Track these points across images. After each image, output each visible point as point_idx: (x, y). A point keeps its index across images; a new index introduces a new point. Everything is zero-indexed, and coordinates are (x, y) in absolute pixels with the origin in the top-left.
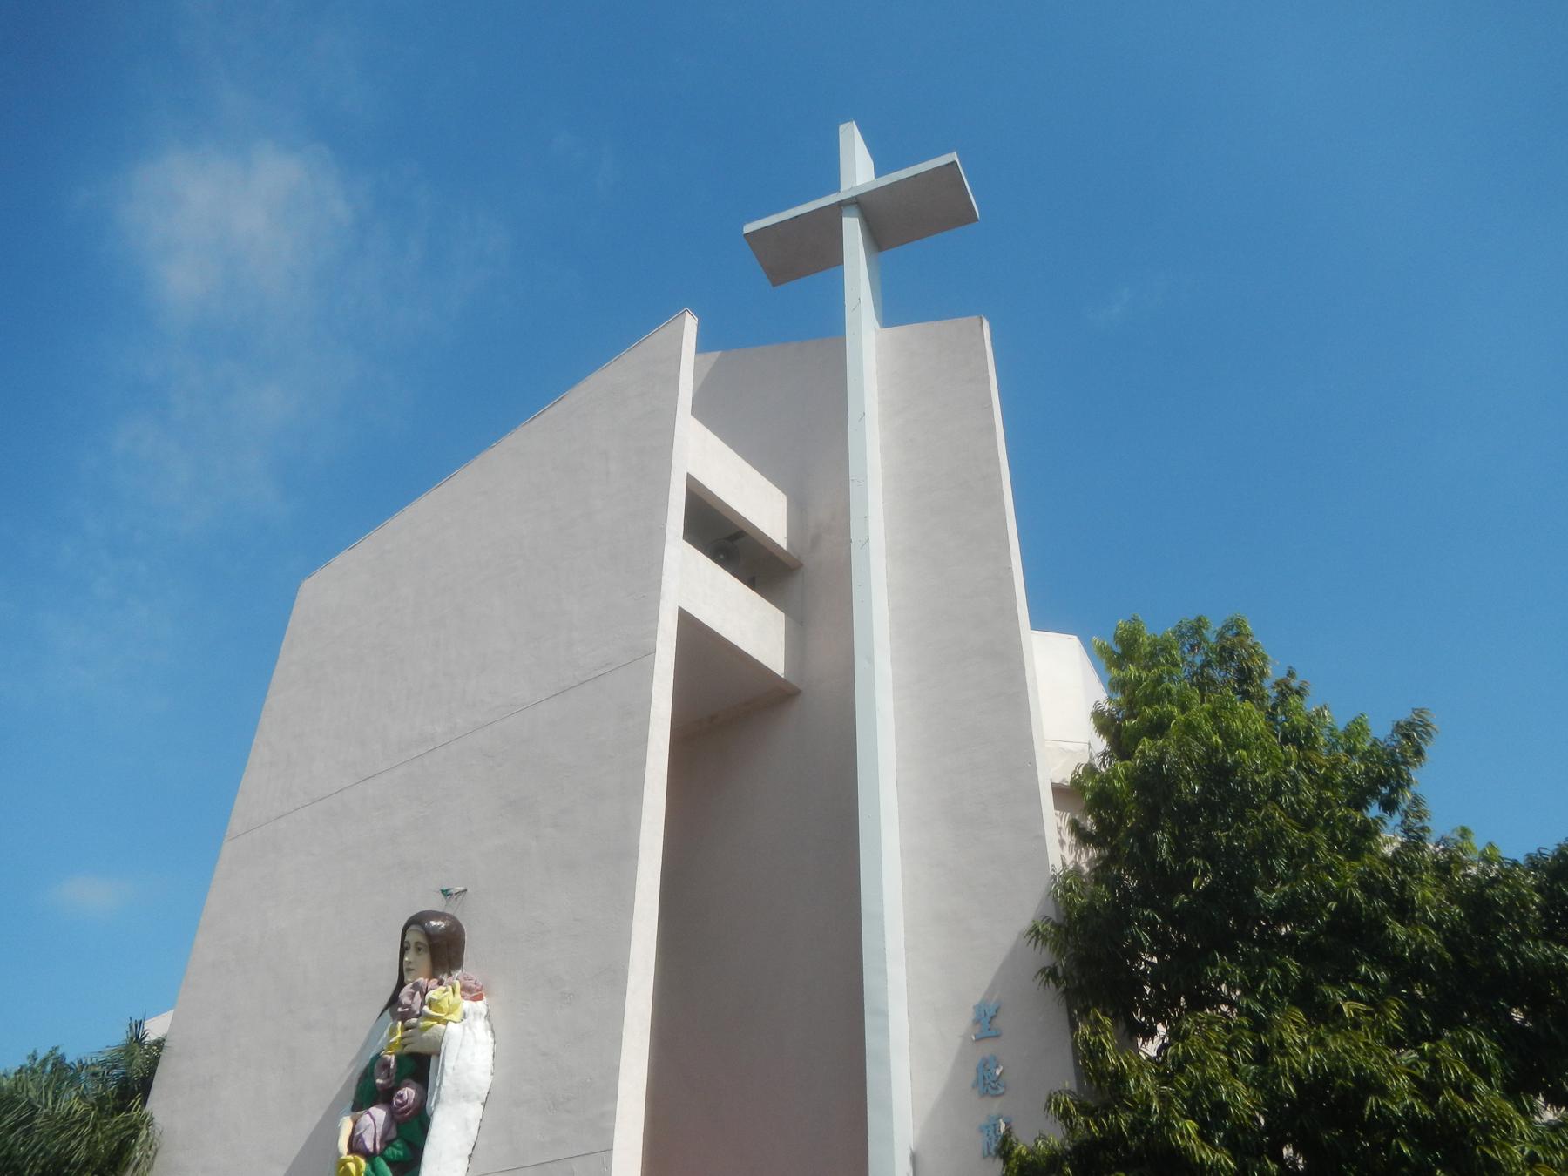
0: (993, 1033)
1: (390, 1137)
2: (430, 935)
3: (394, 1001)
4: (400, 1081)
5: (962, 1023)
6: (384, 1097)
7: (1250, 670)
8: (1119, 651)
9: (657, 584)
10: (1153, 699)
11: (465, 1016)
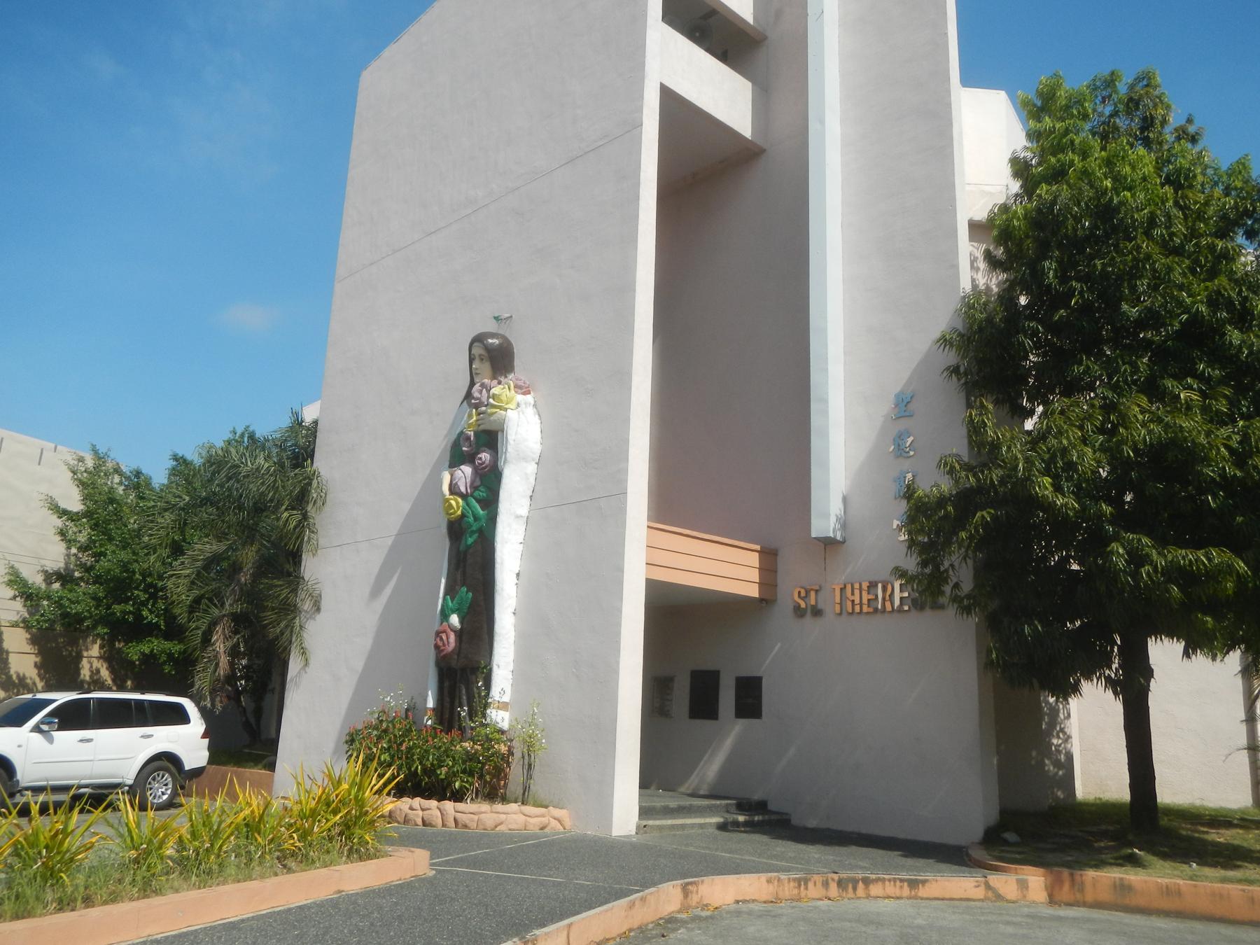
2: (488, 349)
3: (468, 395)
4: (479, 447)
5: (885, 407)
6: (470, 459)
7: (1152, 118)
8: (1039, 103)
9: (641, 66)
10: (1058, 149)
11: (518, 405)
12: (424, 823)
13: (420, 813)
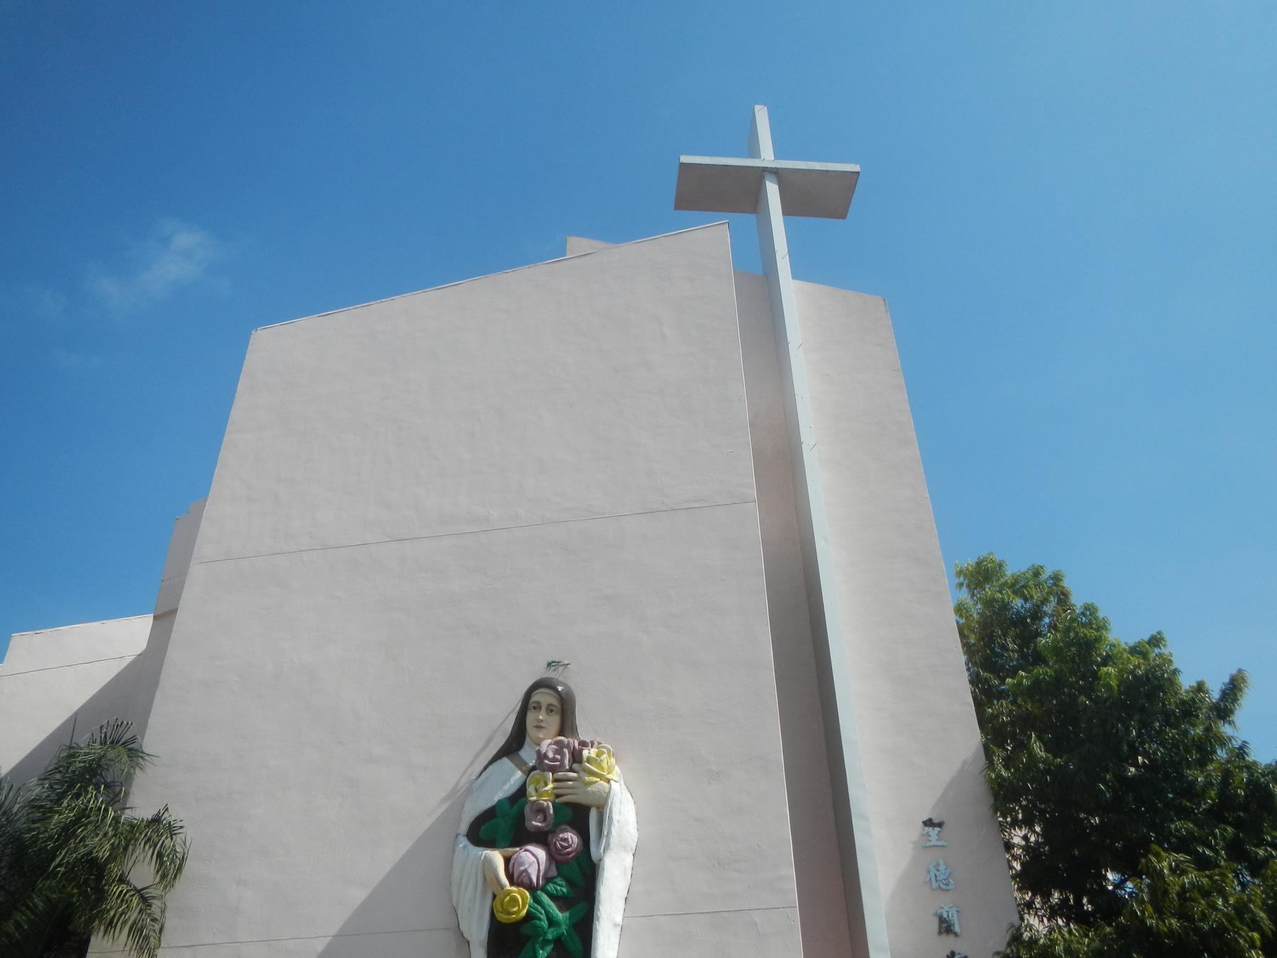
0: (940, 843)
6: (541, 838)
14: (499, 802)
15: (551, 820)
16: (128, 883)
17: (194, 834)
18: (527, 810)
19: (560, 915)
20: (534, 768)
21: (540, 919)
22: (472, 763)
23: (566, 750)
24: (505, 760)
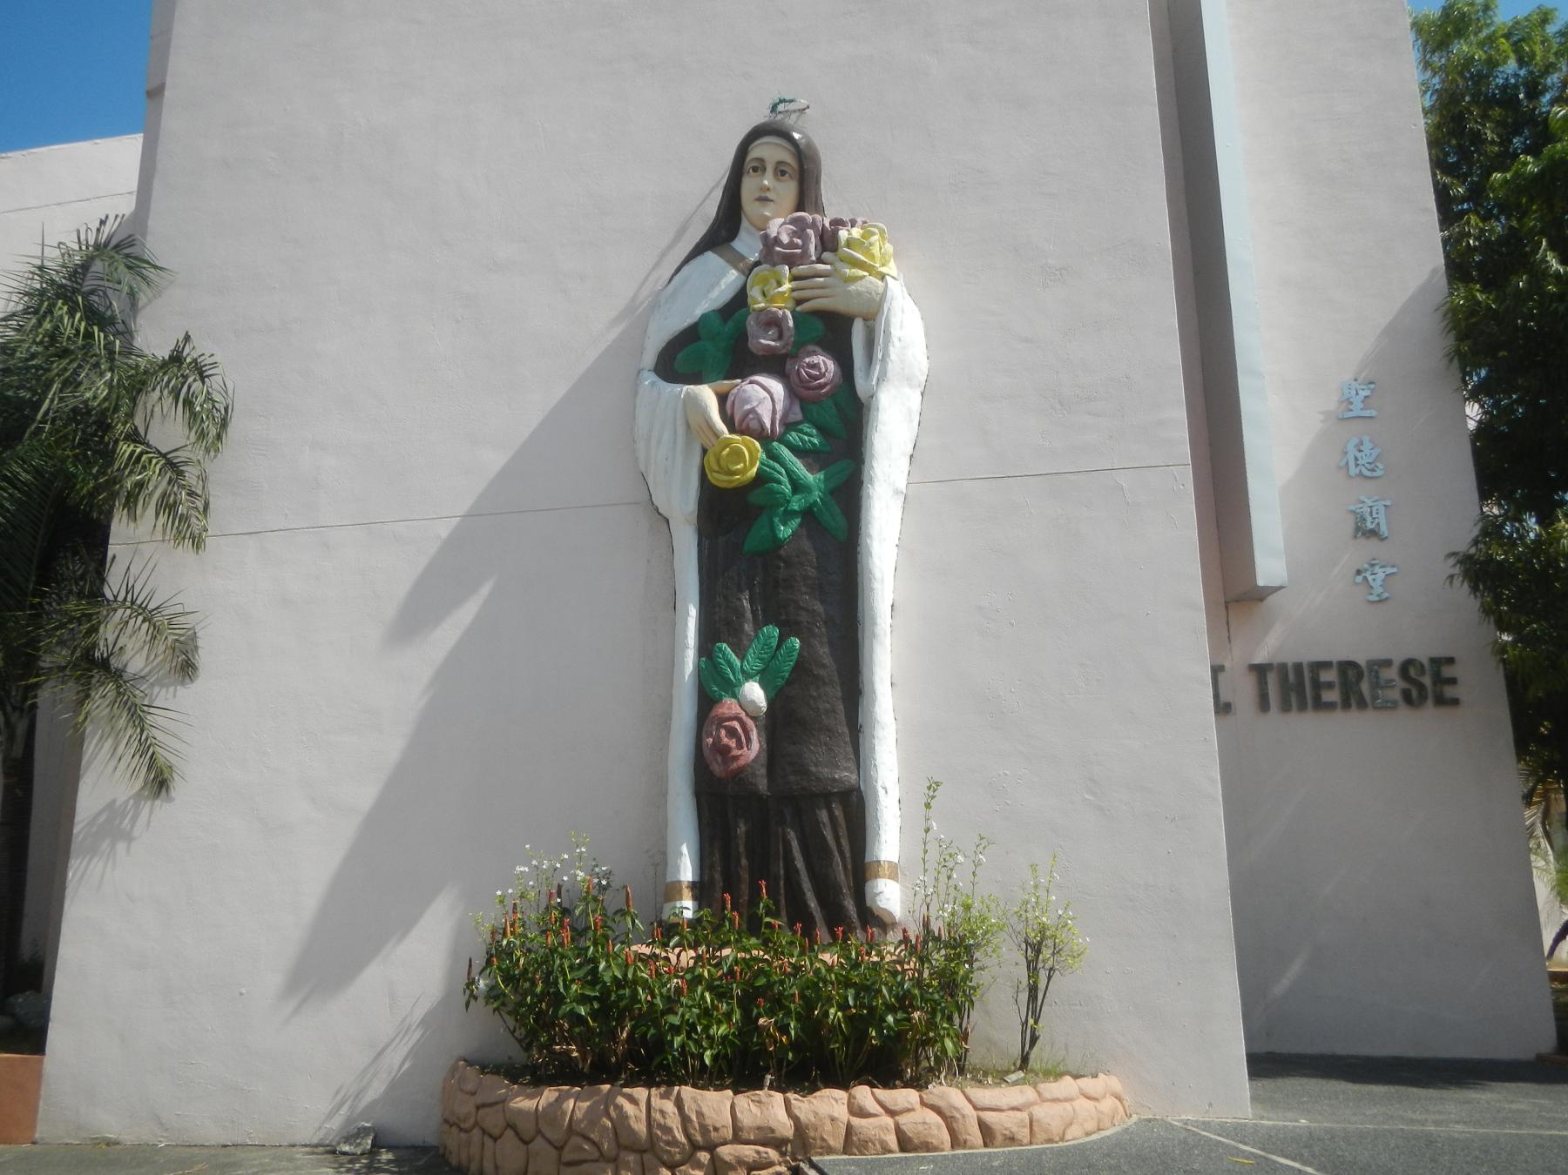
0: (1367, 413)
1: (793, 418)
6: (775, 364)
12: (905, 1143)
13: (889, 1121)
14: (704, 317)
15: (790, 336)
16: (148, 445)
17: (235, 374)
18: (751, 323)
19: (809, 477)
20: (757, 264)
21: (779, 482)
22: (656, 266)
23: (810, 232)
24: (710, 255)
